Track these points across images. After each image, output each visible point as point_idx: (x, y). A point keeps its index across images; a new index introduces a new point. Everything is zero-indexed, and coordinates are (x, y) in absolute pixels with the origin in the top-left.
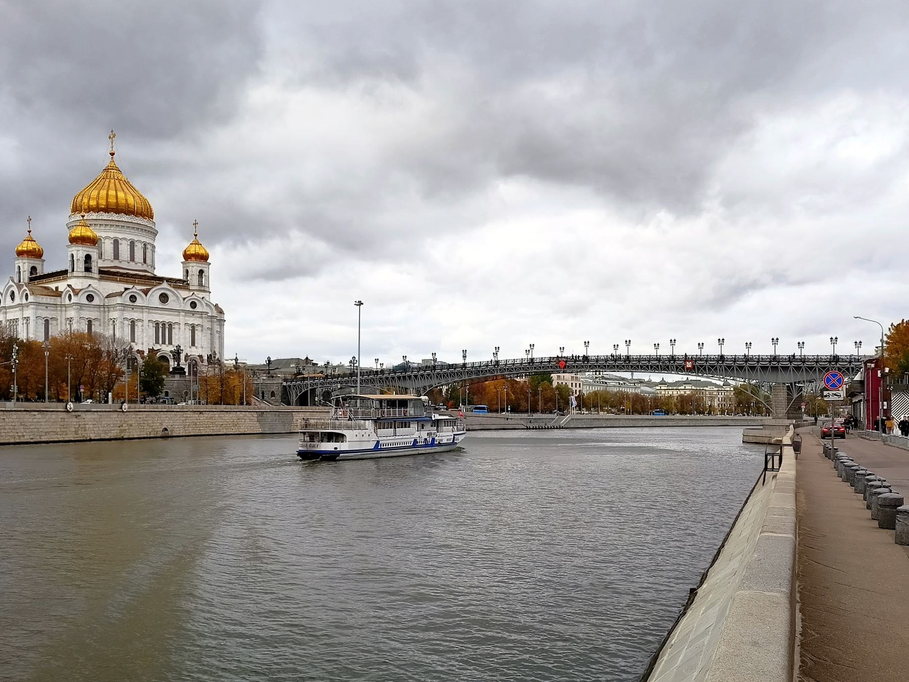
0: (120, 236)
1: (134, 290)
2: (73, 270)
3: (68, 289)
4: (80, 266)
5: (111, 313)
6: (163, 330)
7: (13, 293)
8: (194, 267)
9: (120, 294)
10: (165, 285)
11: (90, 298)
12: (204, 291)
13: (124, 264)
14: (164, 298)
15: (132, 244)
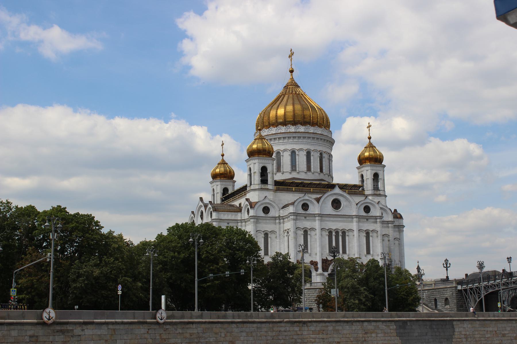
0: (296, 147)
1: (306, 197)
2: (251, 184)
3: (247, 203)
4: (257, 178)
5: (285, 224)
6: (337, 239)
7: (202, 213)
8: (368, 172)
9: (293, 204)
10: (337, 190)
11: (266, 210)
12: (380, 195)
13: (302, 175)
14: (336, 204)
15: (308, 154)
